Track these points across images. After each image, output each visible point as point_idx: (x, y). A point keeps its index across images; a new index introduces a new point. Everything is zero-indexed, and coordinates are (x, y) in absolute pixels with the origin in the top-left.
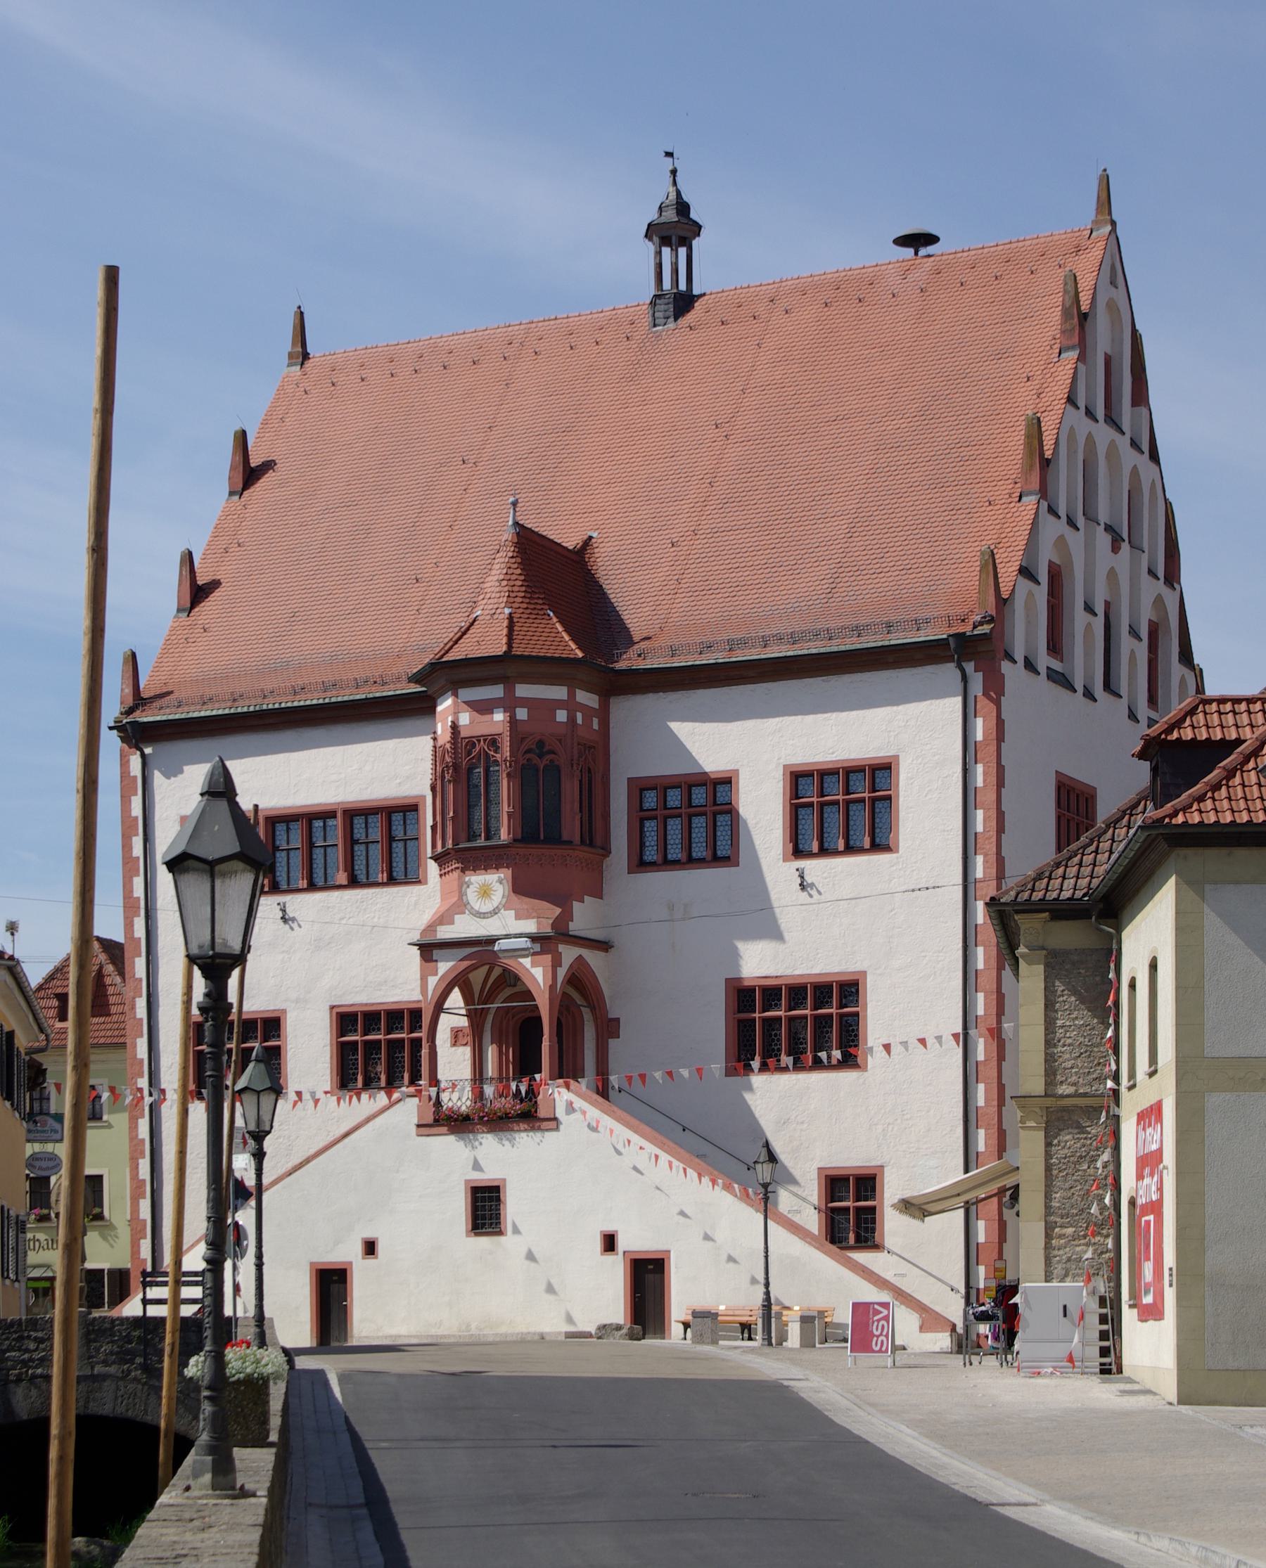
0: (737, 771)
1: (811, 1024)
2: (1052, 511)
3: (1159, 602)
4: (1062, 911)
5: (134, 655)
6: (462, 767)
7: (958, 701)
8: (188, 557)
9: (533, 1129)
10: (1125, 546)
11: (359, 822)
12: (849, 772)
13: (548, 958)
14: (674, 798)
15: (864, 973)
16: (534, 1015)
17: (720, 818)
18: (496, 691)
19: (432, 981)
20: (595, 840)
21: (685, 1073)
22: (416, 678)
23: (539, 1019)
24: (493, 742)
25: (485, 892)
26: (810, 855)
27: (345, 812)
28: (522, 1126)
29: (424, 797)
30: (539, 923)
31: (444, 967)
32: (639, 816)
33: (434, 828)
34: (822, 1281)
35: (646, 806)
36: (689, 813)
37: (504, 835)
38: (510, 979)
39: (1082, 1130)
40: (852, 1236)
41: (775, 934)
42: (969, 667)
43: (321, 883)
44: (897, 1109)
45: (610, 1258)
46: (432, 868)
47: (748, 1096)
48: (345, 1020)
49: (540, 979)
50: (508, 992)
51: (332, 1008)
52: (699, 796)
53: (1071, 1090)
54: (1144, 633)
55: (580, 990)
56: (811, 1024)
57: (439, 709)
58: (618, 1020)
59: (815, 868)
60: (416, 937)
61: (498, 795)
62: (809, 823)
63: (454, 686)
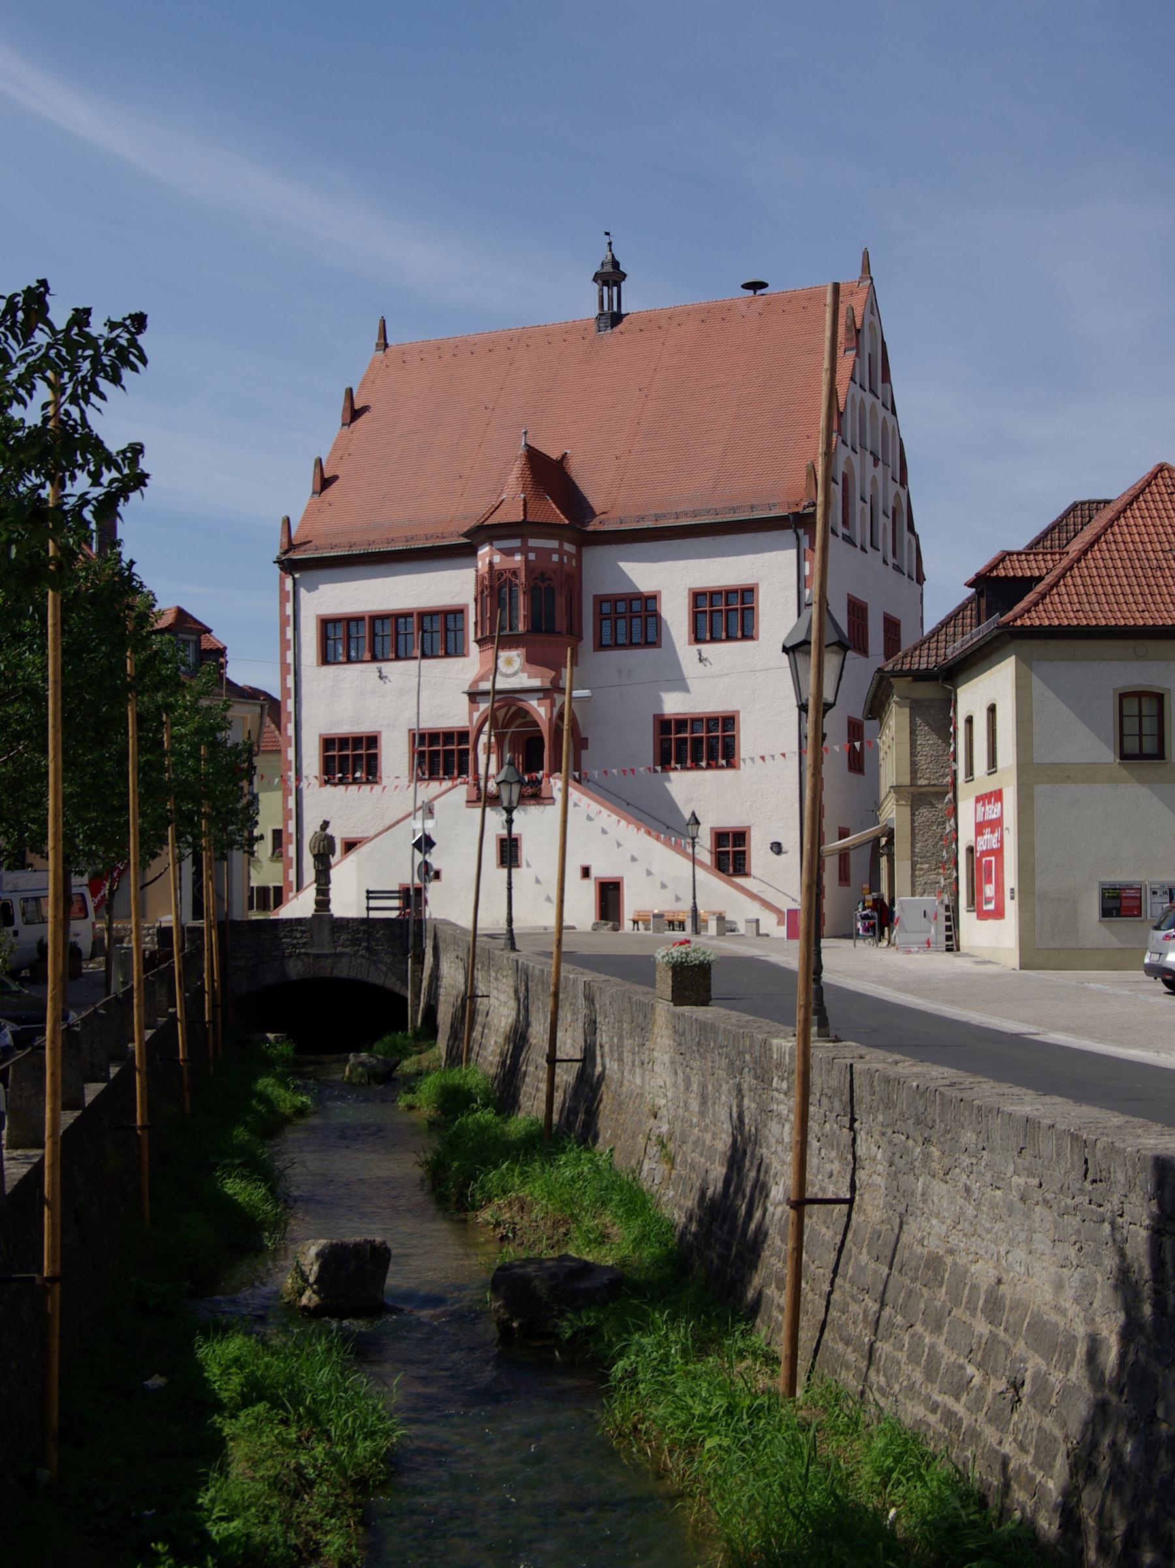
0: (660, 592)
1: (707, 742)
2: (844, 442)
3: (897, 495)
4: (920, 676)
5: (288, 519)
6: (494, 589)
7: (794, 552)
8: (319, 462)
9: (539, 804)
10: (880, 463)
11: (427, 619)
12: (729, 593)
13: (548, 701)
14: (621, 607)
15: (738, 712)
16: (537, 735)
17: (649, 619)
18: (517, 543)
19: (476, 715)
20: (574, 633)
21: (614, 771)
22: (466, 535)
23: (542, 738)
24: (514, 573)
25: (509, 662)
26: (705, 641)
27: (419, 613)
28: (532, 802)
29: (467, 605)
31: (484, 706)
32: (600, 617)
33: (476, 623)
34: (717, 893)
35: (604, 611)
36: (630, 616)
37: (521, 628)
38: (523, 714)
39: (933, 806)
40: (731, 868)
41: (685, 689)
42: (801, 532)
43: (380, 657)
44: (761, 791)
45: (586, 881)
46: (474, 648)
47: (667, 785)
49: (543, 714)
50: (520, 721)
52: (636, 606)
53: (926, 782)
54: (890, 514)
56: (707, 742)
57: (480, 553)
58: (587, 739)
59: (708, 649)
60: (466, 689)
61: (517, 604)
62: (705, 622)
63: (490, 540)
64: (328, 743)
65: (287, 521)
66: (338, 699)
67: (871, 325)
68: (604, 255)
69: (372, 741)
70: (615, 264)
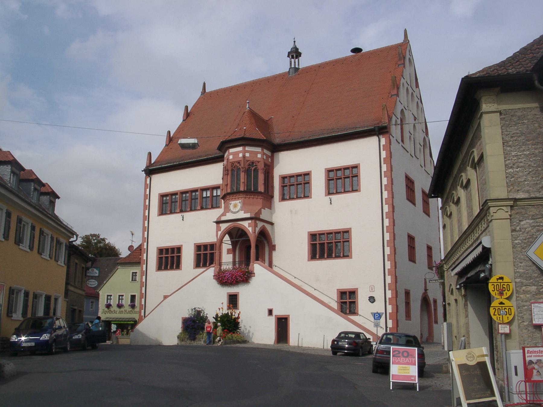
19: (219, 233)
24: (239, 162)
26: (333, 194)
30: (251, 214)
48: (198, 247)
59: (334, 197)
60: (215, 220)
64: (161, 251)
65: (150, 154)
66: (168, 230)
67: (409, 59)
68: (292, 46)
69: (179, 249)
70: (297, 49)
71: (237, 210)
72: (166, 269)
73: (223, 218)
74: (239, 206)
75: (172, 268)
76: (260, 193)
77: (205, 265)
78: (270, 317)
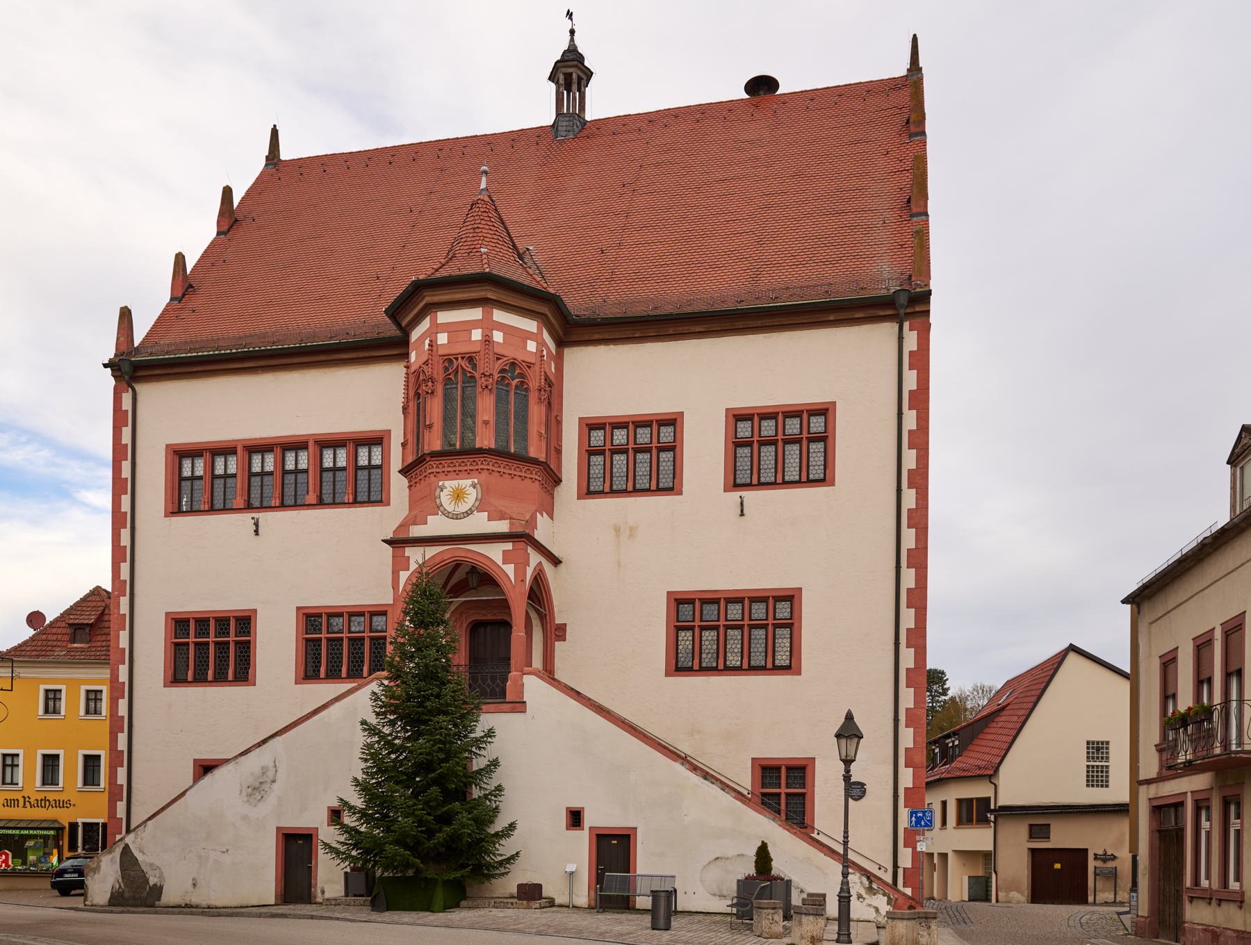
19: (404, 576)
33: (404, 445)
46: (398, 485)
51: (298, 609)
55: (538, 594)
60: (389, 536)
71: (461, 507)
72: (200, 679)
73: (417, 531)
74: (472, 496)
75: (220, 678)
76: (535, 462)
77: (355, 673)
78: (575, 833)
